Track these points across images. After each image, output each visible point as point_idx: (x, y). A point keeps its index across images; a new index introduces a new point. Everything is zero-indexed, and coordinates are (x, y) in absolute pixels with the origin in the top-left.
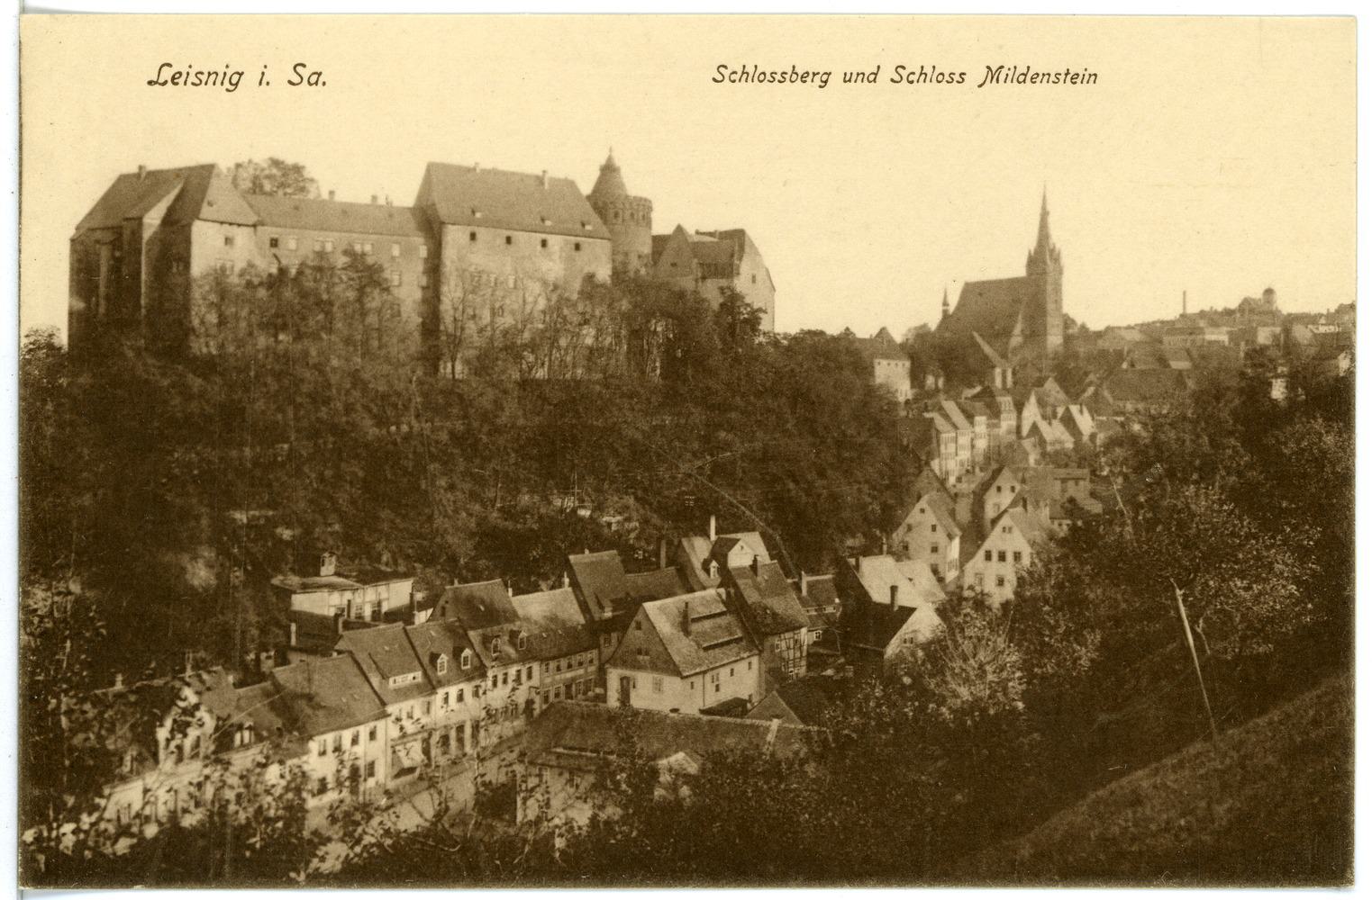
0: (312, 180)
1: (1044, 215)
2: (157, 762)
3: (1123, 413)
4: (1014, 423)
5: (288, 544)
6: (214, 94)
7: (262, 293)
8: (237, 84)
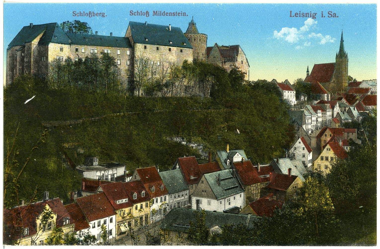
0: (90, 28)
2: (37, 231)
3: (368, 110)
5: (82, 154)
7: (73, 67)
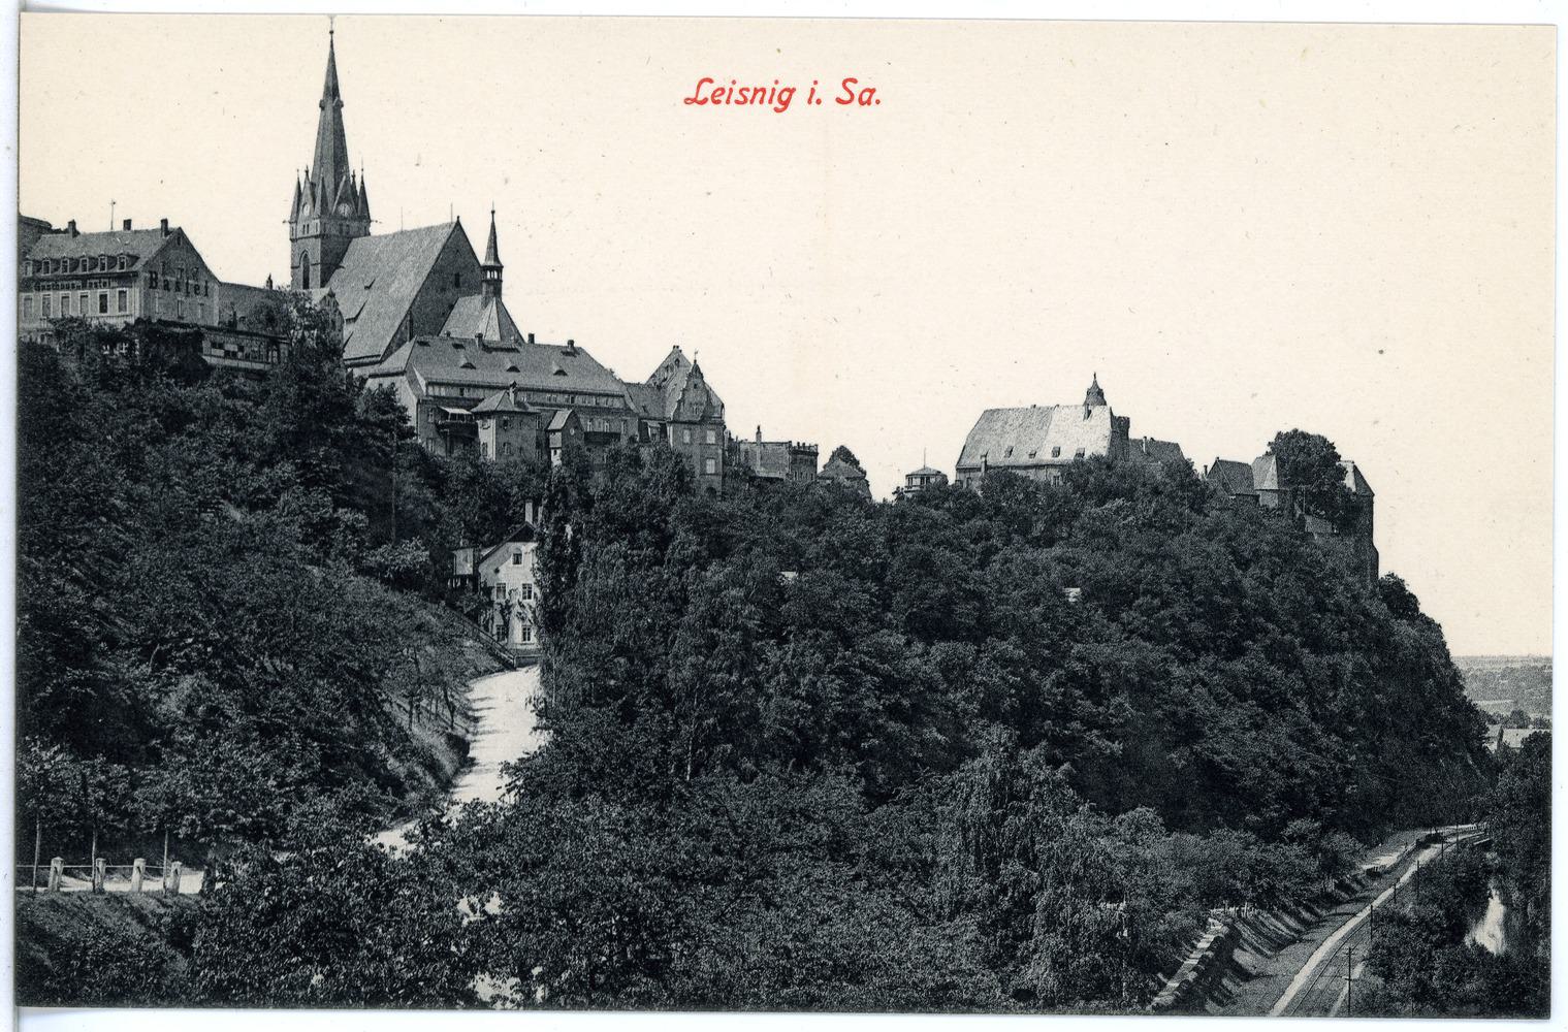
6: (764, 111)
8: (786, 104)
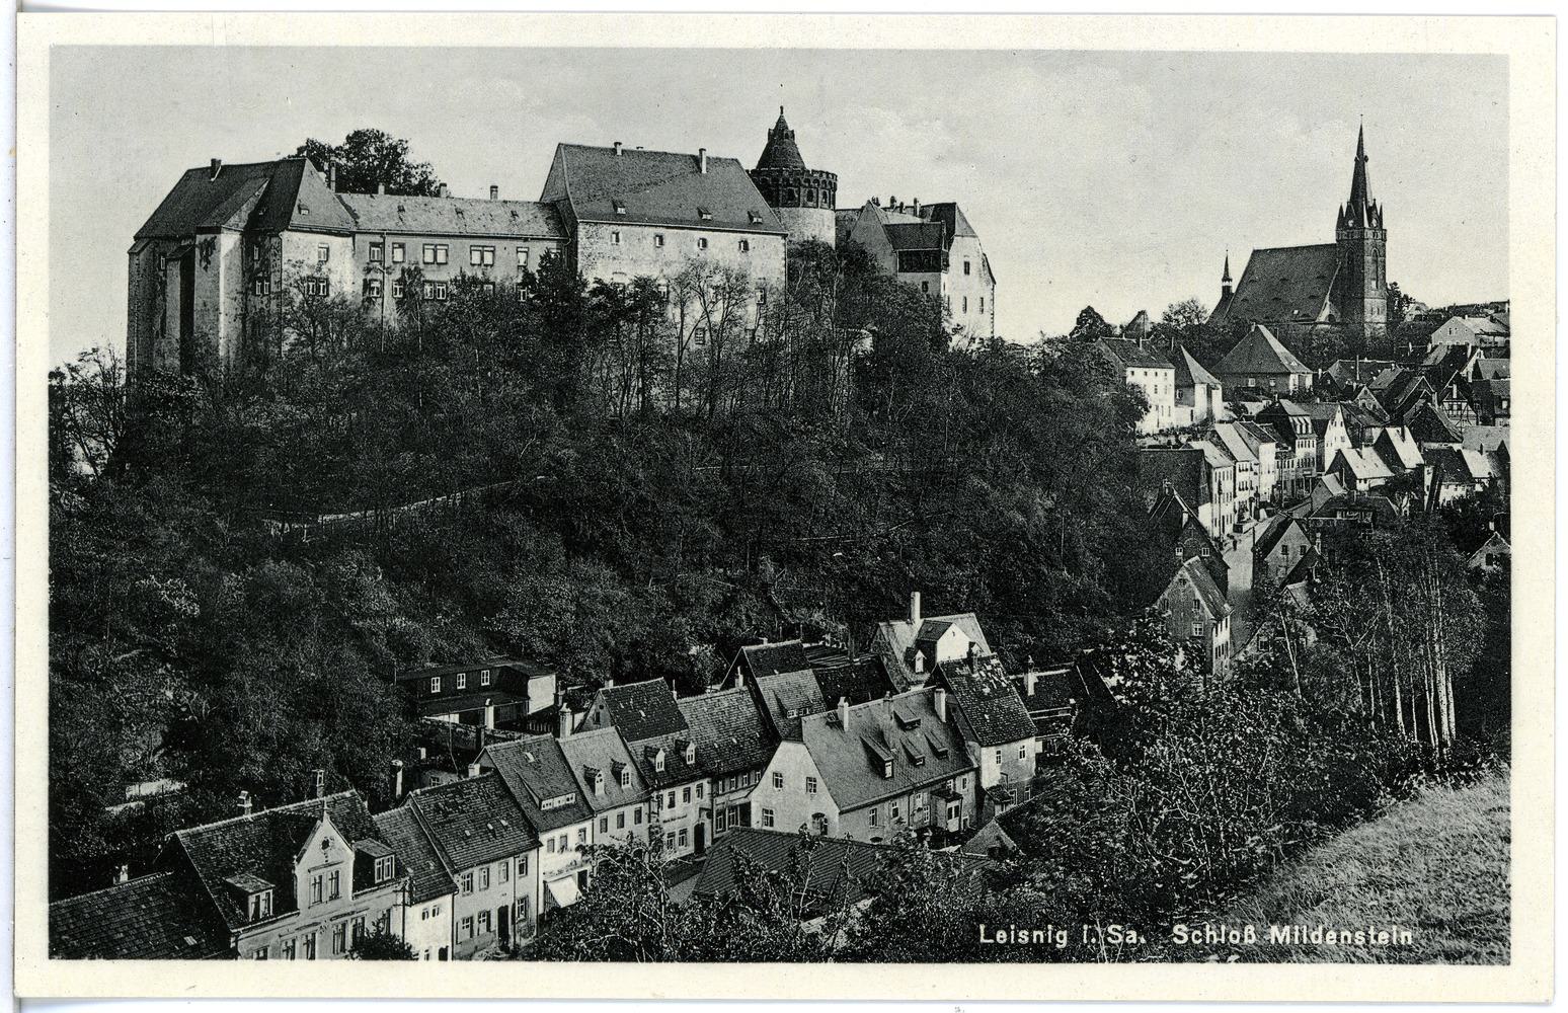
1: (1361, 160)
4: (1313, 451)
